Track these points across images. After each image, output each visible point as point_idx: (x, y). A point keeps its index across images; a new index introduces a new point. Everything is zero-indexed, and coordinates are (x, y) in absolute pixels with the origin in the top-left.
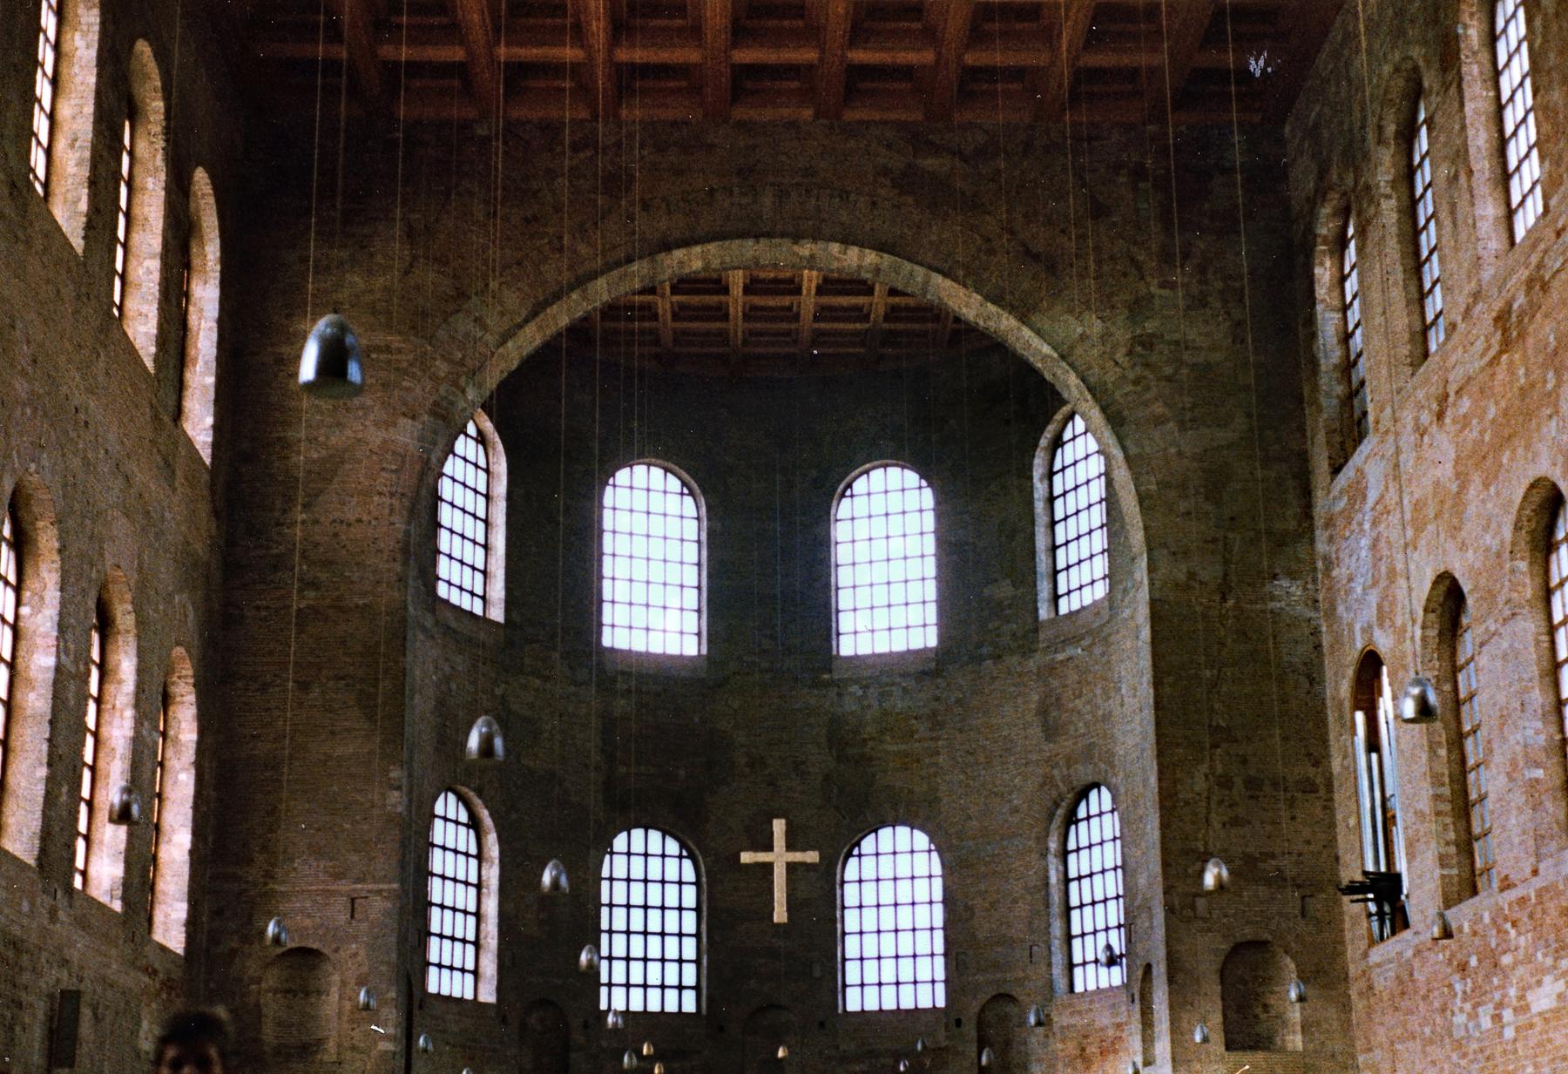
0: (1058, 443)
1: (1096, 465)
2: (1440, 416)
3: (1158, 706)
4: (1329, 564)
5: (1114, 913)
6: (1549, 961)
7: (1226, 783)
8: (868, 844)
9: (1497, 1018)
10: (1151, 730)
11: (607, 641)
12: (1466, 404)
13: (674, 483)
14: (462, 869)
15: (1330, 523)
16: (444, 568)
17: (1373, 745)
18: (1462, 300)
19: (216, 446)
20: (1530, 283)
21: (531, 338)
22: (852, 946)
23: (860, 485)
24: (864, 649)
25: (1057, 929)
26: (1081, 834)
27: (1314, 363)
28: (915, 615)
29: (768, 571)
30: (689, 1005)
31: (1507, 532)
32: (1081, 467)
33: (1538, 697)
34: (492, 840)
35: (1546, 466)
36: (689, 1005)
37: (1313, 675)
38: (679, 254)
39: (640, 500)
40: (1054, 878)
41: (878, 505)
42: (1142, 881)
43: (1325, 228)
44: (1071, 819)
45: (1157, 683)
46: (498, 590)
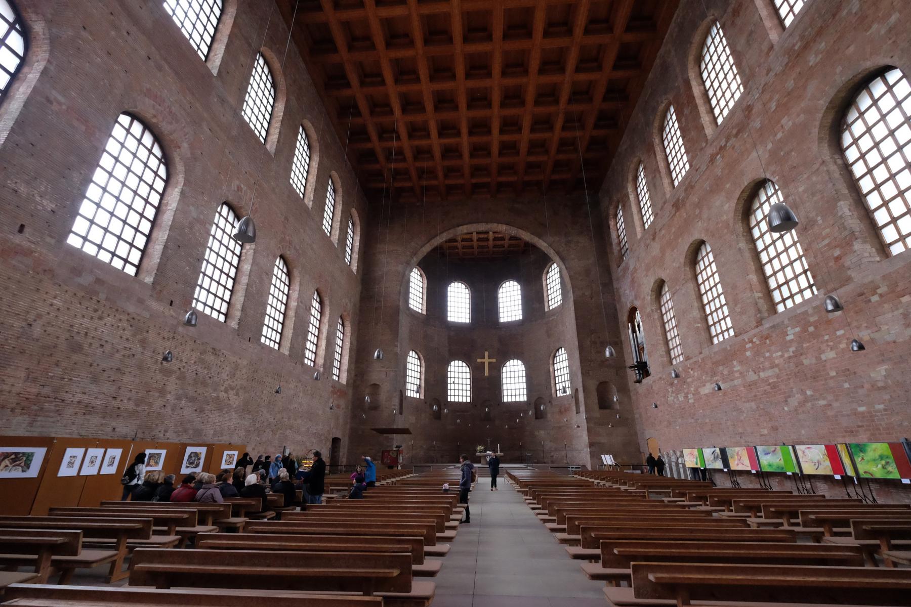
0: (548, 272)
1: (558, 275)
2: (654, 239)
3: (577, 324)
4: (618, 289)
5: (567, 377)
6: (708, 378)
7: (595, 343)
8: (508, 364)
9: (686, 397)
10: (575, 331)
11: (449, 319)
12: (663, 232)
13: (464, 286)
14: (414, 368)
15: (618, 279)
16: (411, 301)
17: (634, 331)
18: (660, 206)
19: (357, 270)
20: (686, 190)
21: (427, 248)
22: (505, 387)
23: (504, 285)
24: (506, 320)
25: (552, 382)
26: (558, 359)
27: (611, 244)
28: (517, 313)
29: (484, 305)
30: (468, 400)
31: (682, 260)
32: (553, 279)
33: (696, 304)
34: (423, 362)
35: (697, 236)
36: (468, 400)
37: (614, 317)
38: (460, 228)
39: (456, 290)
40: (551, 370)
41: (508, 289)
42: (574, 368)
43: (611, 212)
44: (555, 356)
45: (577, 319)
46: (425, 308)
